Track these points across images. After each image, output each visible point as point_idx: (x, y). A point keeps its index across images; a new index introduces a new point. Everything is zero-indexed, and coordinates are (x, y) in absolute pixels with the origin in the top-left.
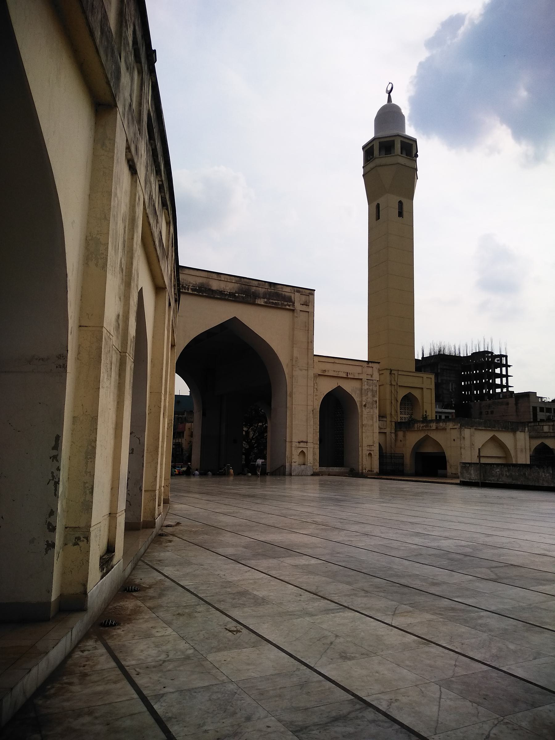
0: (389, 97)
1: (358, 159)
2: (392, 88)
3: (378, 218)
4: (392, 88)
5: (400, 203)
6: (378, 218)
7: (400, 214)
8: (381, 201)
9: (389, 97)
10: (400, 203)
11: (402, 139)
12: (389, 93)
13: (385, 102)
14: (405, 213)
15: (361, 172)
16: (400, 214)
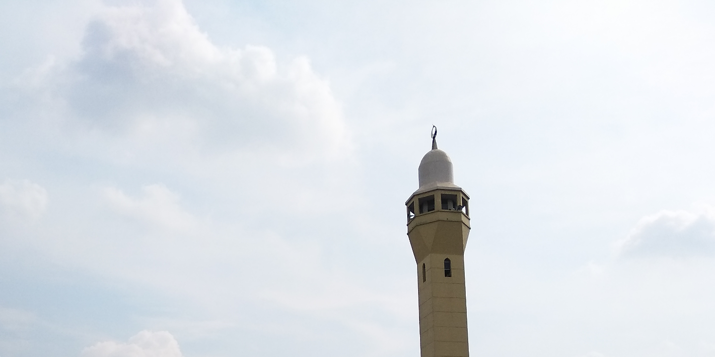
0: (434, 141)
1: (401, 215)
2: (436, 132)
3: (425, 280)
4: (436, 132)
5: (447, 263)
6: (425, 280)
7: (448, 273)
8: (426, 261)
9: (434, 141)
10: (447, 263)
11: (443, 193)
12: (434, 138)
13: (429, 149)
14: (453, 272)
15: (406, 230)
16: (448, 273)
